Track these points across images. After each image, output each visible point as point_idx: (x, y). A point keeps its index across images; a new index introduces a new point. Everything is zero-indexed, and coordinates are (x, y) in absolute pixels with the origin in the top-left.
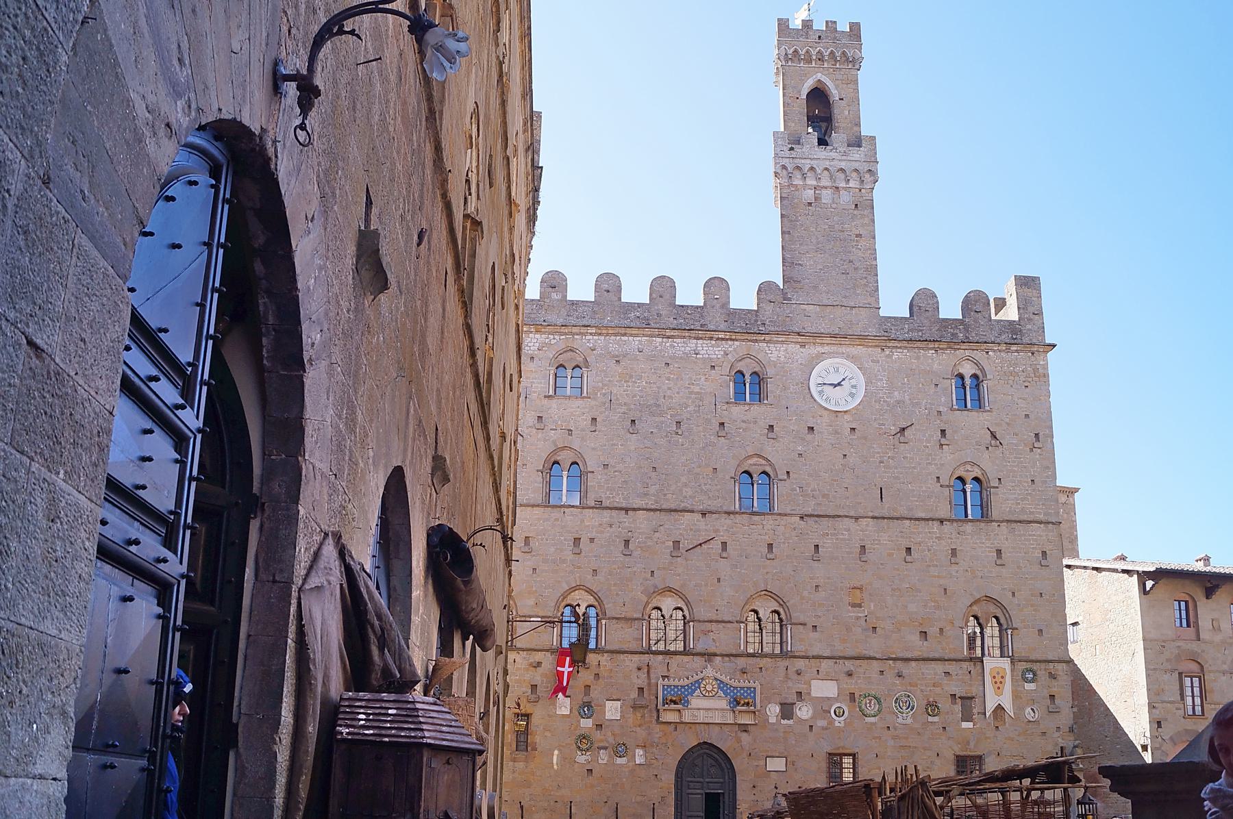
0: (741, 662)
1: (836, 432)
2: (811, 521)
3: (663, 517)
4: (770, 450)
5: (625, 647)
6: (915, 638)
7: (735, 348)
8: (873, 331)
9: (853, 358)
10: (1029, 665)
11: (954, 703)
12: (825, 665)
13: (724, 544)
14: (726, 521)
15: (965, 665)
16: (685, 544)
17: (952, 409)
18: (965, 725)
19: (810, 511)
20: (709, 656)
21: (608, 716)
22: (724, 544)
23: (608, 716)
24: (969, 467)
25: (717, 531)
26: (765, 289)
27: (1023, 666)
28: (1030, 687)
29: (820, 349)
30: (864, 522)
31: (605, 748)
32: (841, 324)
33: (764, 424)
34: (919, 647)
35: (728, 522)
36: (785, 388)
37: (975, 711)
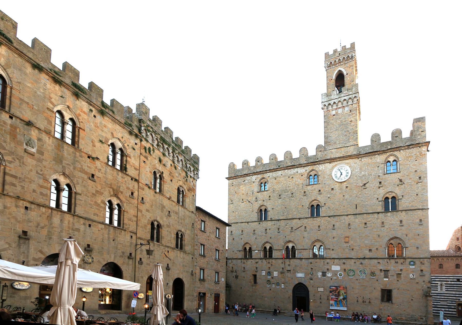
1: (341, 189)
3: (288, 221)
4: (319, 198)
5: (279, 257)
8: (355, 153)
9: (347, 164)
10: (412, 260)
13: (305, 227)
14: (306, 220)
15: (386, 260)
16: (294, 228)
19: (332, 215)
22: (305, 227)
25: (303, 223)
28: (411, 267)
29: (336, 163)
32: (344, 153)
33: (317, 190)
34: (369, 255)
35: (307, 220)
36: (324, 178)
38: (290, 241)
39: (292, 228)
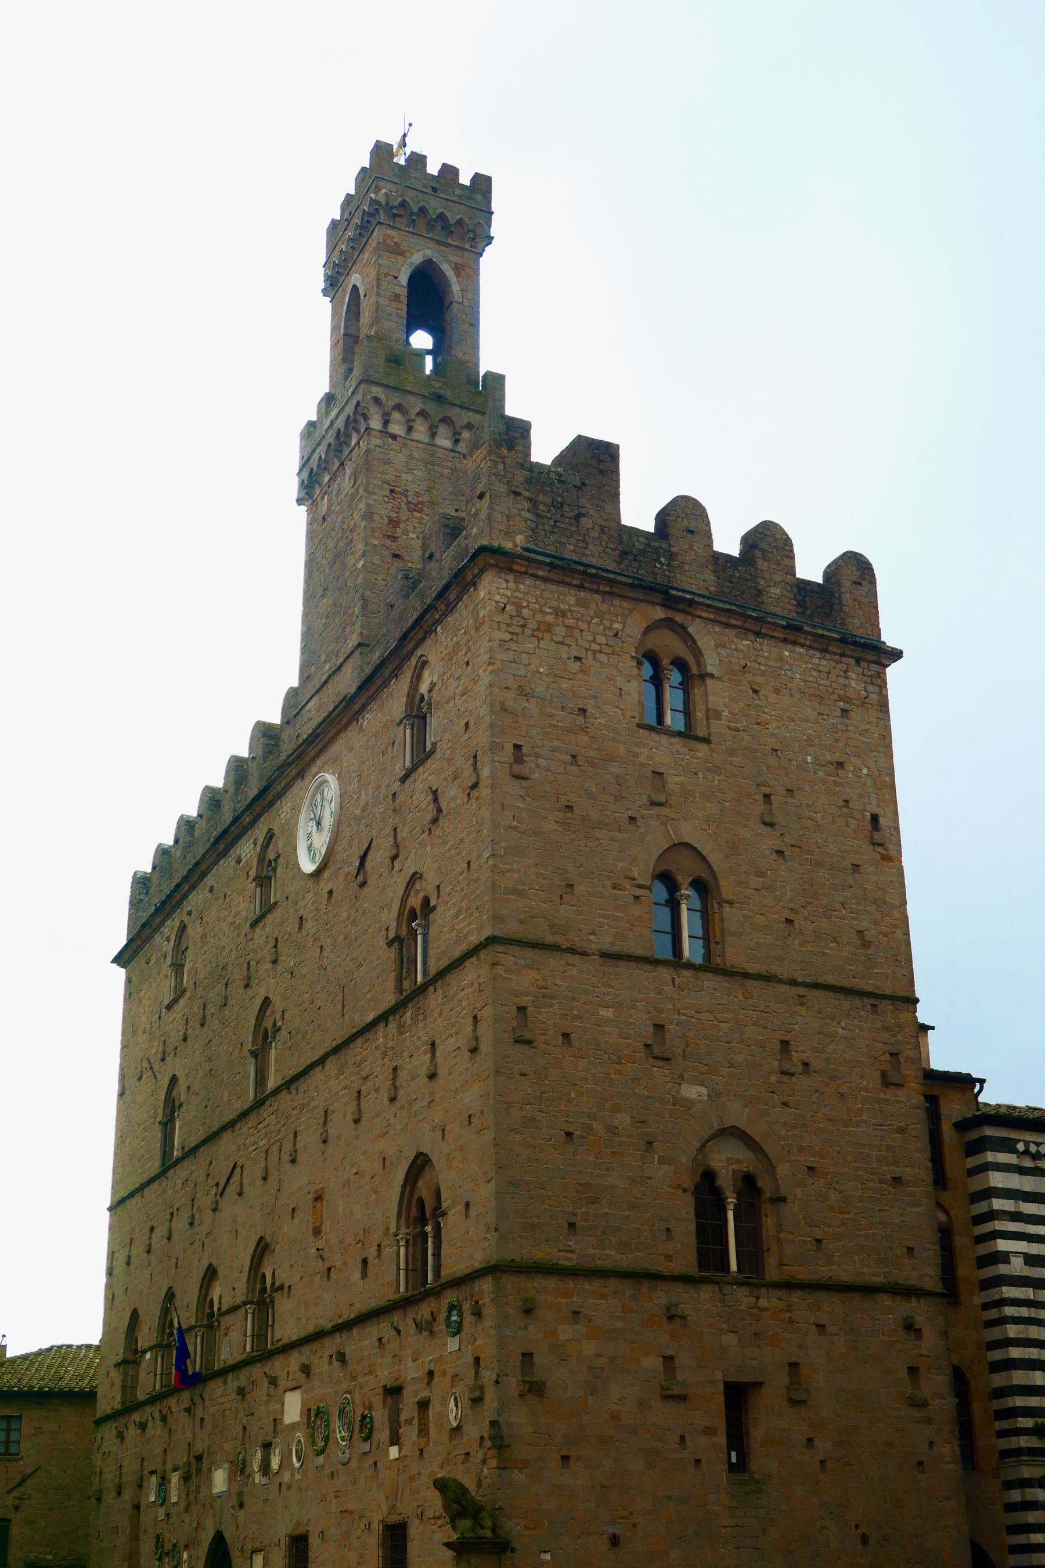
0: (243, 1378)
2: (293, 1087)
6: (357, 1275)
7: (259, 832)
11: (384, 1402)
12: (295, 1360)
14: (244, 1128)
17: (403, 780)
18: (394, 1452)
20: (224, 1372)
21: (174, 1499)
23: (174, 1499)
24: (417, 886)
26: (294, 703)
27: (450, 1297)
28: (453, 1344)
30: (328, 1065)
31: (167, 1554)
37: (402, 1419)
38: (211, 1274)
39: (217, 1184)
